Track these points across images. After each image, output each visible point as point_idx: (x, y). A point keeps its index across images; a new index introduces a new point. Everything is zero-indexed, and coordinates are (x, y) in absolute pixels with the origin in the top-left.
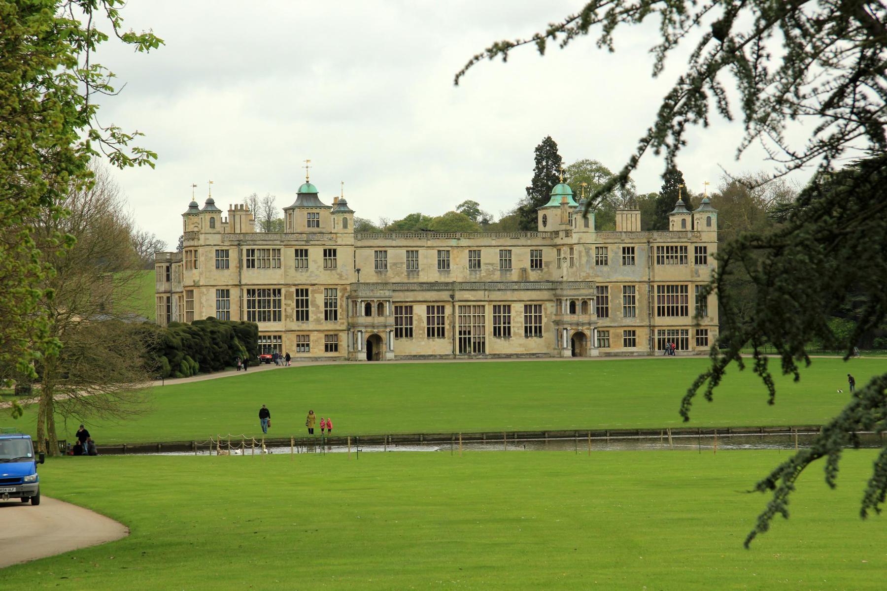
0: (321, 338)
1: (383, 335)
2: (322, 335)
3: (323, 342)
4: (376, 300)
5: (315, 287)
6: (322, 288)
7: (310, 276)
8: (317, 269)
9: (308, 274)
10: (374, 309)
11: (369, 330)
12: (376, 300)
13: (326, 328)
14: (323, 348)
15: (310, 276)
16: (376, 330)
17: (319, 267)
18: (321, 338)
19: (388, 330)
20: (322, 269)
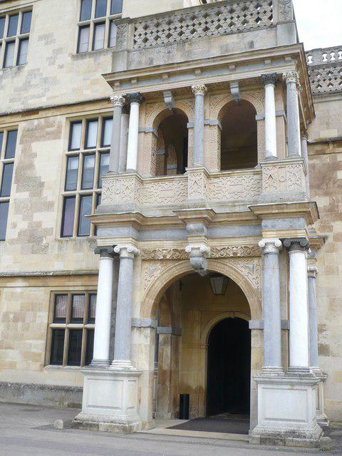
0: (33, 307)
1: (241, 273)
2: (42, 295)
3: (42, 319)
4: (198, 83)
5: (35, 121)
6: (61, 120)
7: (27, 85)
8: (52, 61)
9: (20, 80)
10: (205, 142)
11: (164, 244)
12: (198, 83)
13: (58, 266)
14: (39, 345)
15: (27, 85)
16: (197, 247)
17: (58, 51)
18: (33, 307)
19: (271, 240)
20: (65, 59)
